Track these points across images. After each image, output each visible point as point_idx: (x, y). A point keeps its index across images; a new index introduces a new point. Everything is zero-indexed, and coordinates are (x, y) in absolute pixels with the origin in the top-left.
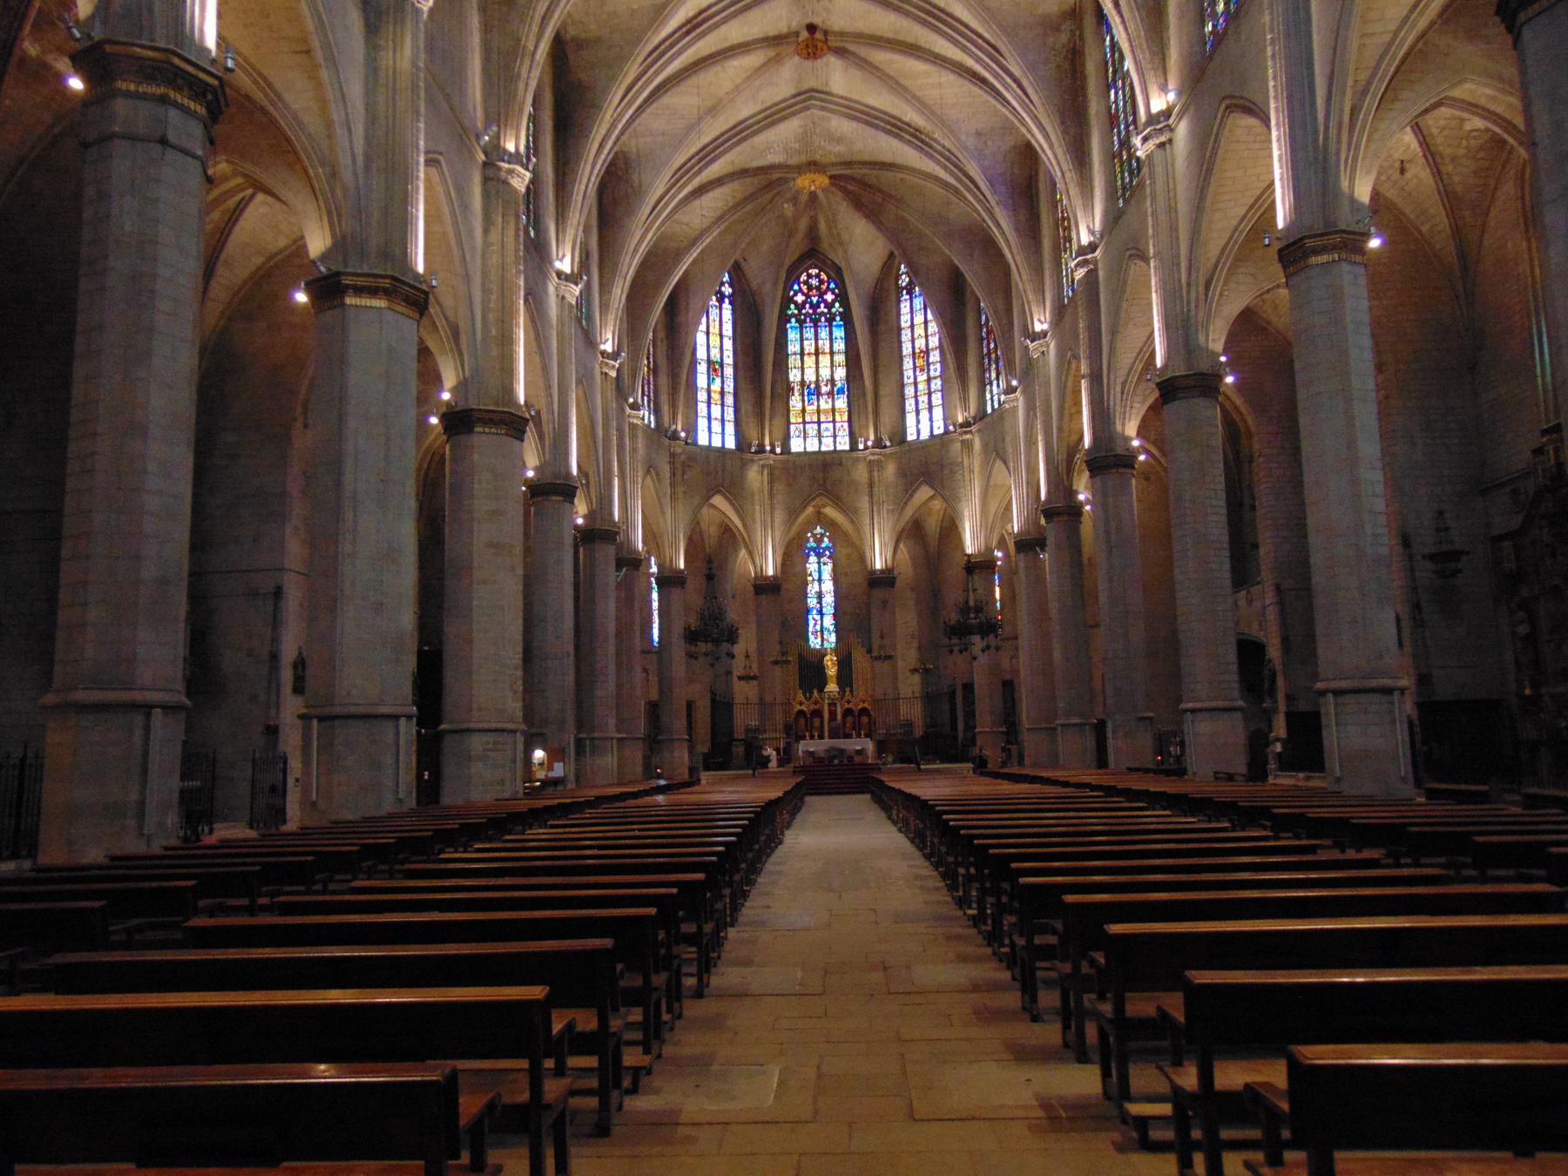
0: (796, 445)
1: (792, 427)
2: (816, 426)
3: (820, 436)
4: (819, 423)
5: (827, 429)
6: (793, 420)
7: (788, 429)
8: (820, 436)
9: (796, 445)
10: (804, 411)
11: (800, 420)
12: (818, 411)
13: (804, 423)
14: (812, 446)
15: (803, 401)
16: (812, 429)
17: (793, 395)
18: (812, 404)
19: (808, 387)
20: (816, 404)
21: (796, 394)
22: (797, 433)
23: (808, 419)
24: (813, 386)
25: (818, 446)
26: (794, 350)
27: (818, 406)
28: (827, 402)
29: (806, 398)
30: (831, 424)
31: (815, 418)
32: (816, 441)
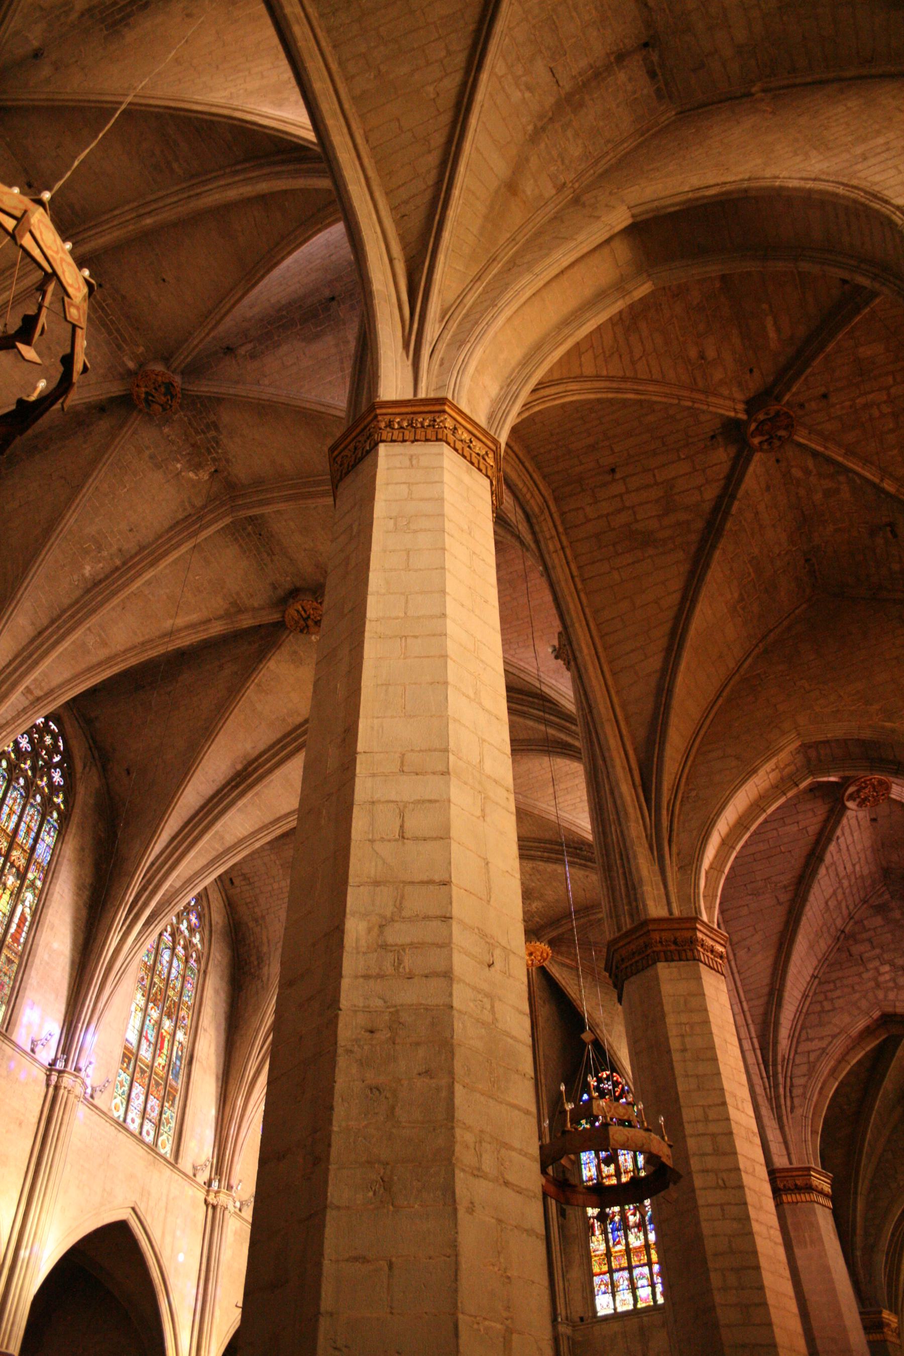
0: (604, 1305)
1: (596, 1280)
2: (626, 1274)
3: (633, 1288)
4: (630, 1268)
5: (642, 1276)
6: (596, 1269)
7: (592, 1282)
8: (633, 1288)
9: (604, 1305)
10: (608, 1254)
11: (605, 1268)
12: (628, 1251)
13: (611, 1271)
14: (625, 1302)
15: (607, 1241)
16: (622, 1278)
17: (593, 1234)
18: (619, 1243)
19: (612, 1221)
20: (623, 1242)
21: (597, 1232)
22: (603, 1288)
23: (614, 1265)
24: (617, 1218)
25: (632, 1302)
26: (589, 1174)
27: (627, 1244)
28: (637, 1238)
29: (610, 1236)
30: (646, 1270)
31: (625, 1263)
32: (629, 1297)
